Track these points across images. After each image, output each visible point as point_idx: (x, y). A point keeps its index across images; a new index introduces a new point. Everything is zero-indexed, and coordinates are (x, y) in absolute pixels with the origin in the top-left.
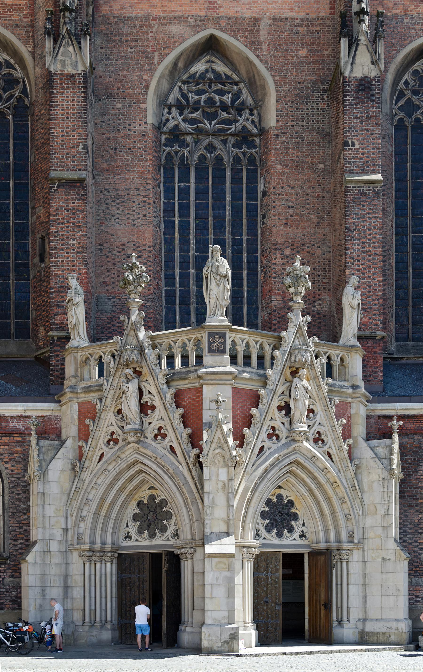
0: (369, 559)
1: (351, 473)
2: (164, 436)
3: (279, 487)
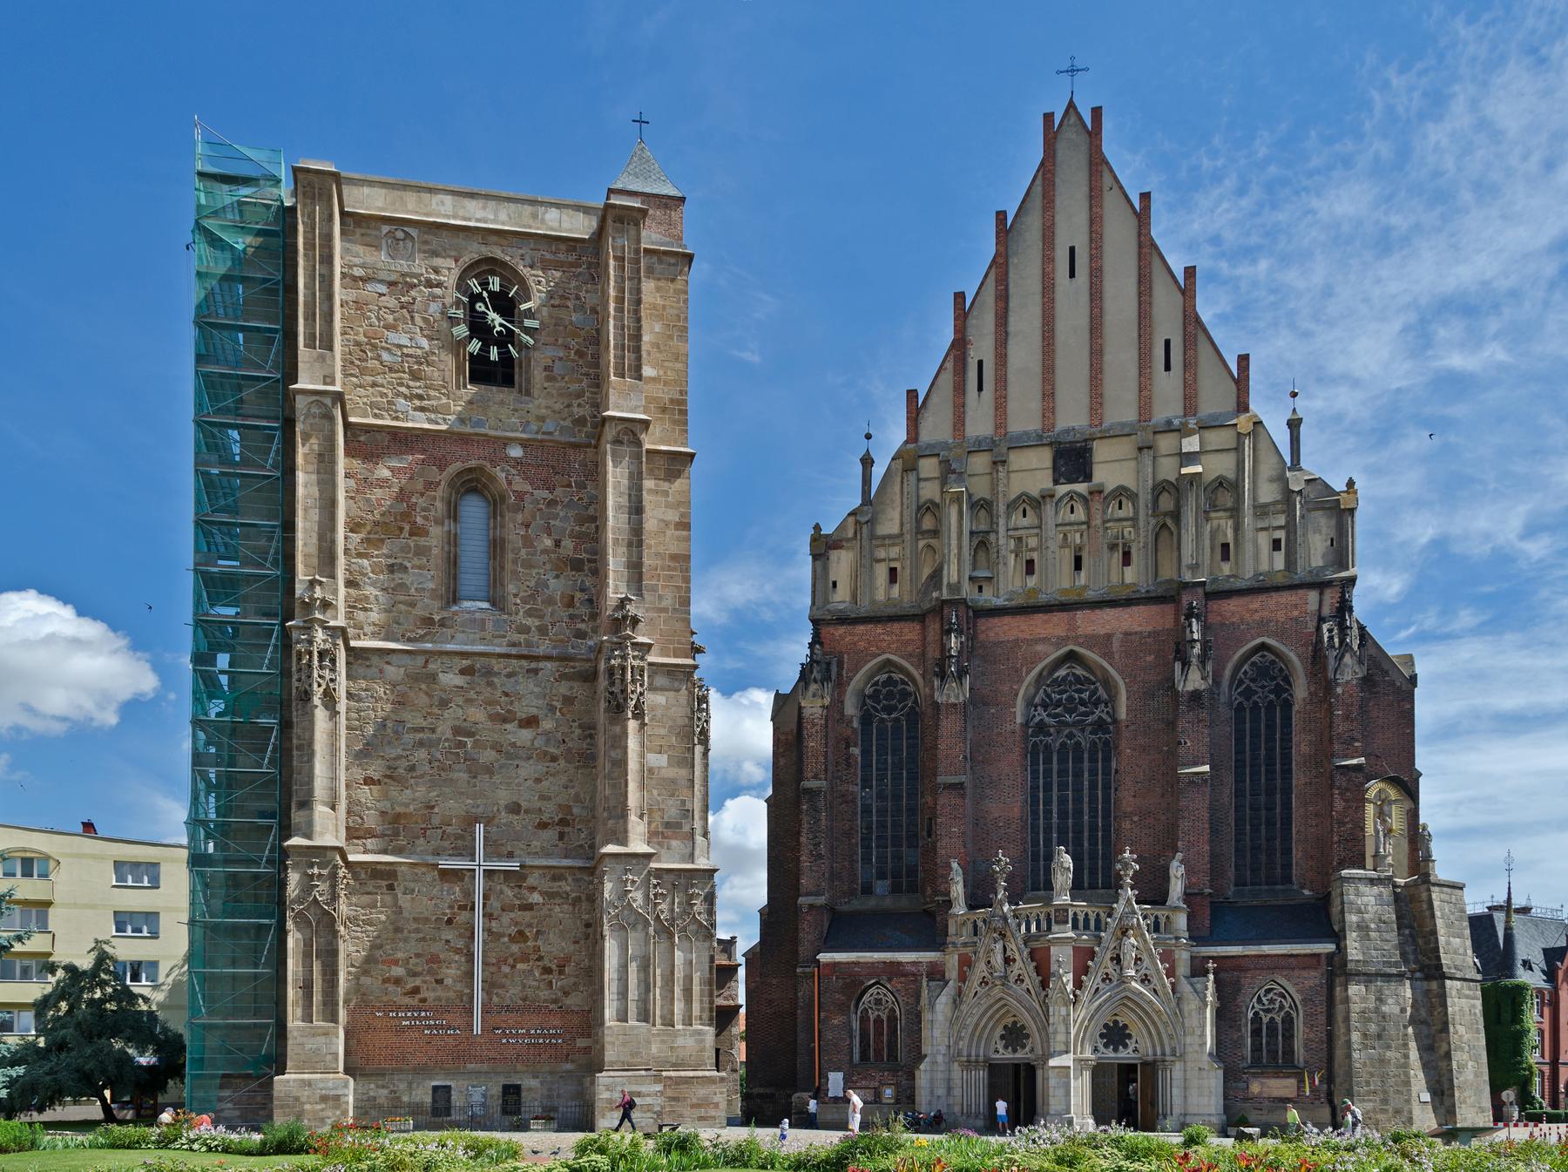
0: (1189, 1069)
1: (1174, 1004)
2: (1022, 981)
3: (1116, 1015)
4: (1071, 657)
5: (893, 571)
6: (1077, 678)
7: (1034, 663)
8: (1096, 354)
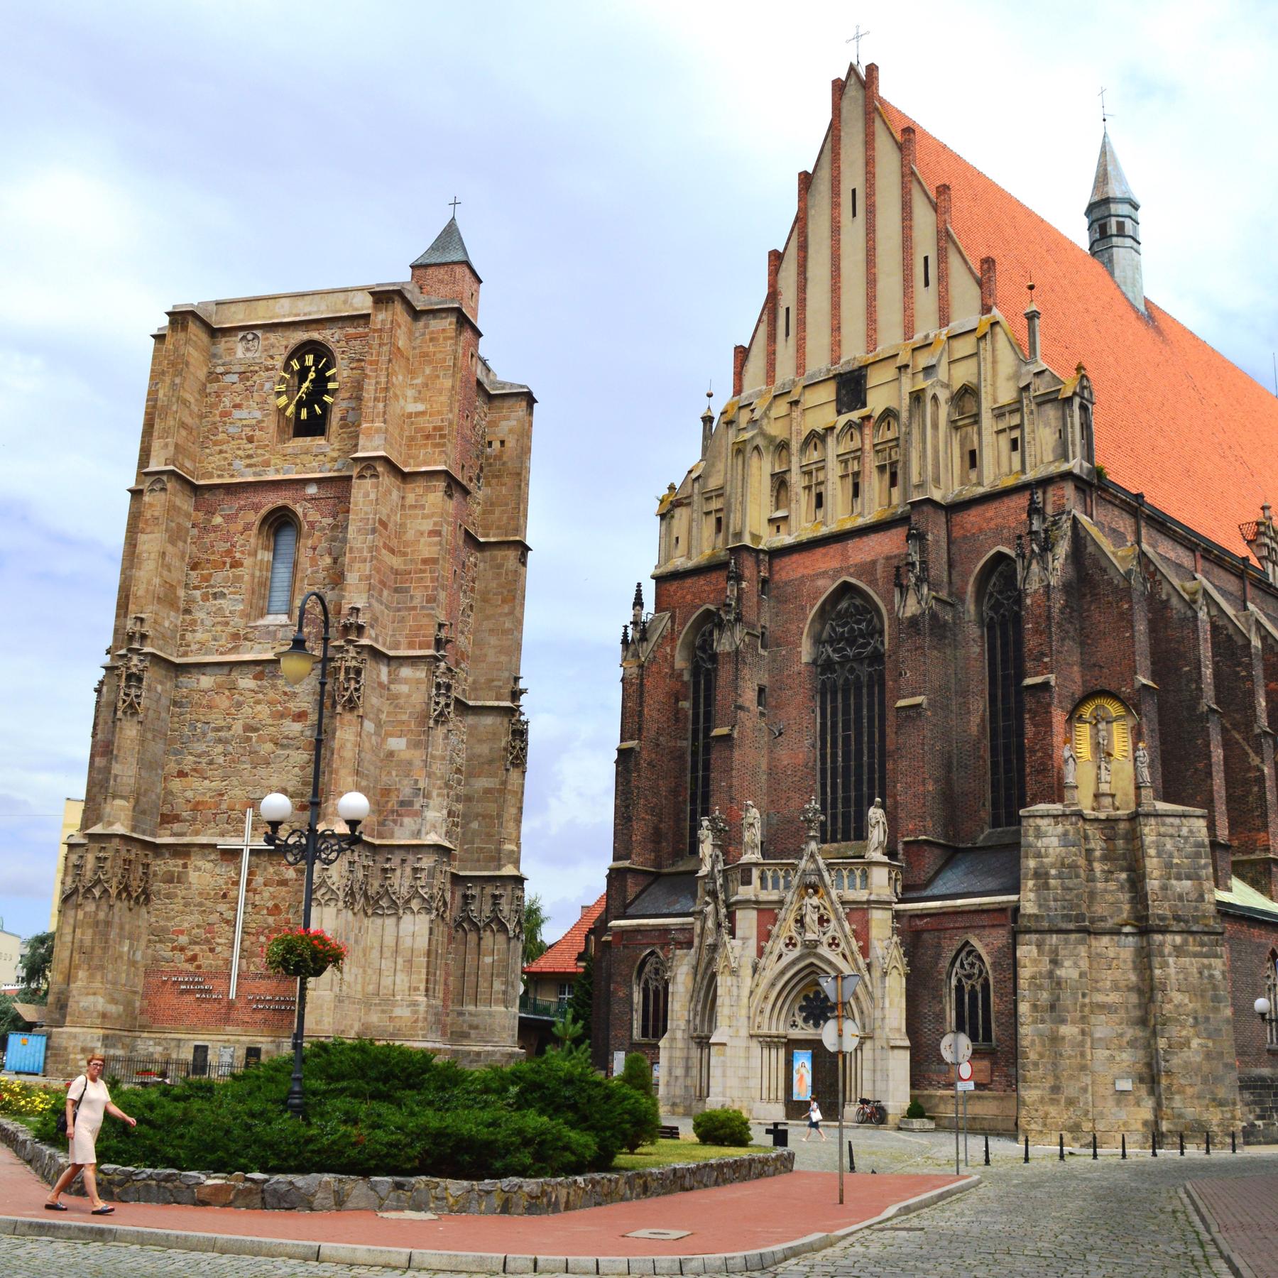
4: (846, 589)
5: (719, 520)
6: (856, 607)
7: (816, 599)
8: (871, 281)
